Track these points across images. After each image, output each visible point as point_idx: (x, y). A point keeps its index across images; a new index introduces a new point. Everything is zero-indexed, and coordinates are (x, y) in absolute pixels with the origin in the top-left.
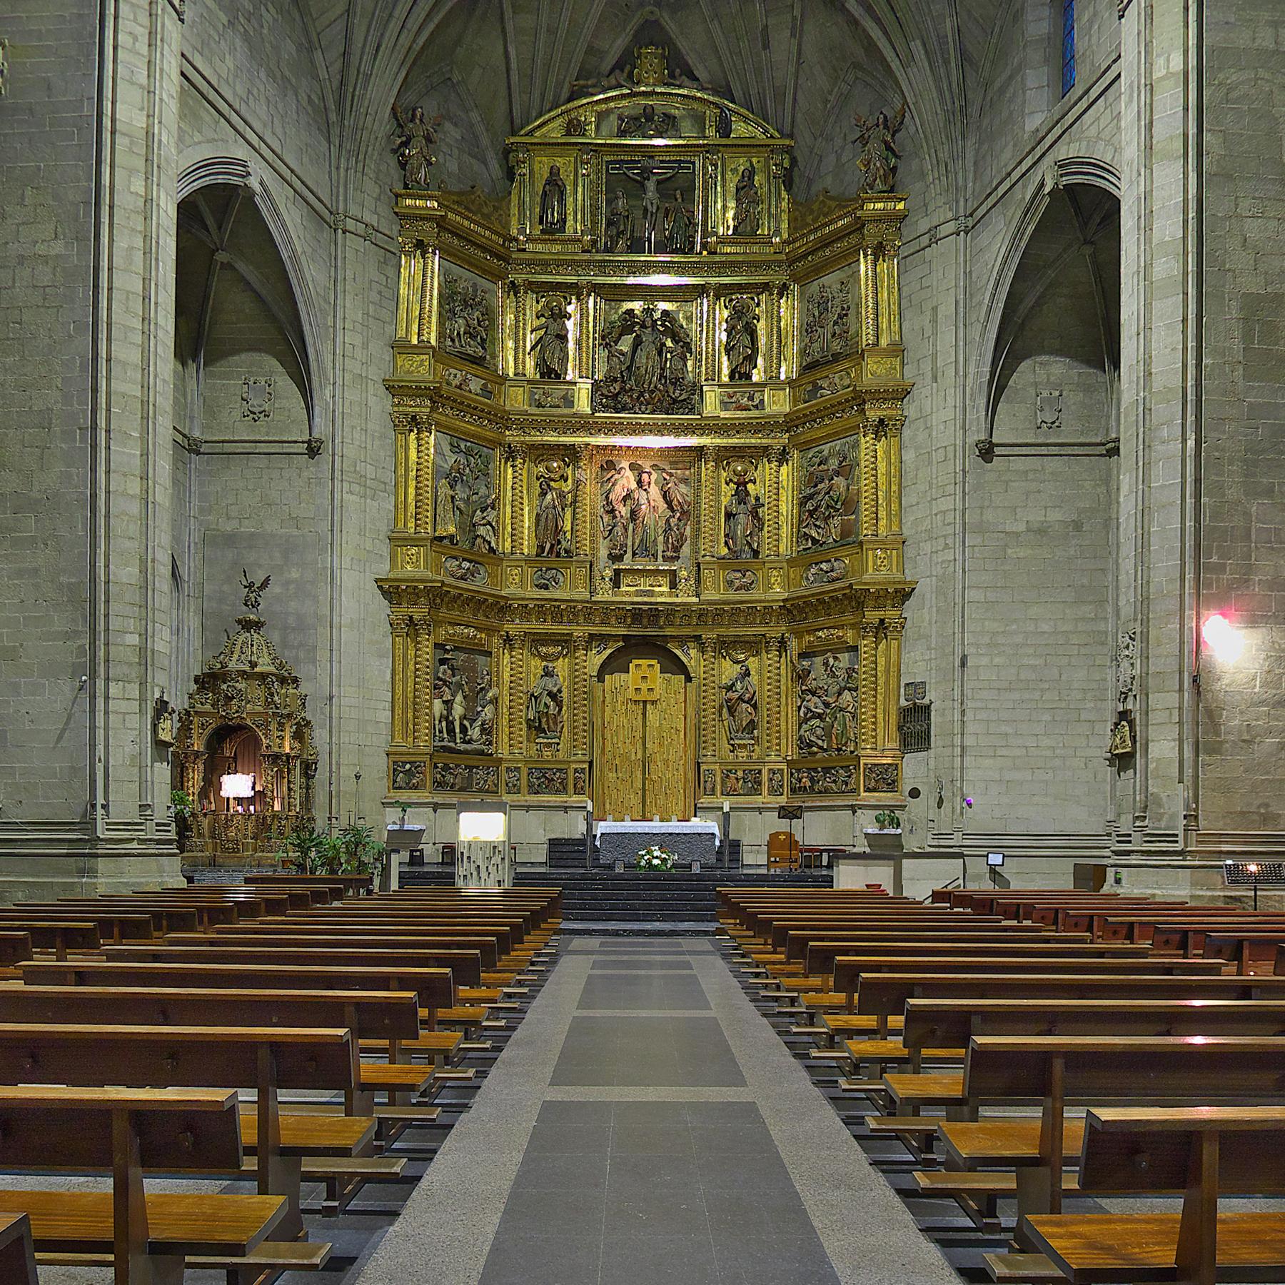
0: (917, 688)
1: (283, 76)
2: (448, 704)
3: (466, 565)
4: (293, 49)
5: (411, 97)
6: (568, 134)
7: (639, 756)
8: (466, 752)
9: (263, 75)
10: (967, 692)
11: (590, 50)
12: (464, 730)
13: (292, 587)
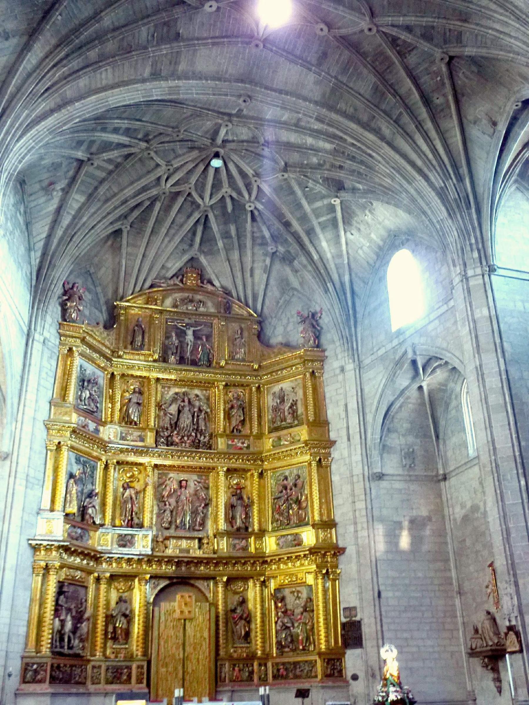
2: (63, 623)
3: (79, 531)
5: (72, 277)
6: (147, 303)
7: (181, 656)
8: (69, 655)
10: (383, 613)
11: (163, 267)
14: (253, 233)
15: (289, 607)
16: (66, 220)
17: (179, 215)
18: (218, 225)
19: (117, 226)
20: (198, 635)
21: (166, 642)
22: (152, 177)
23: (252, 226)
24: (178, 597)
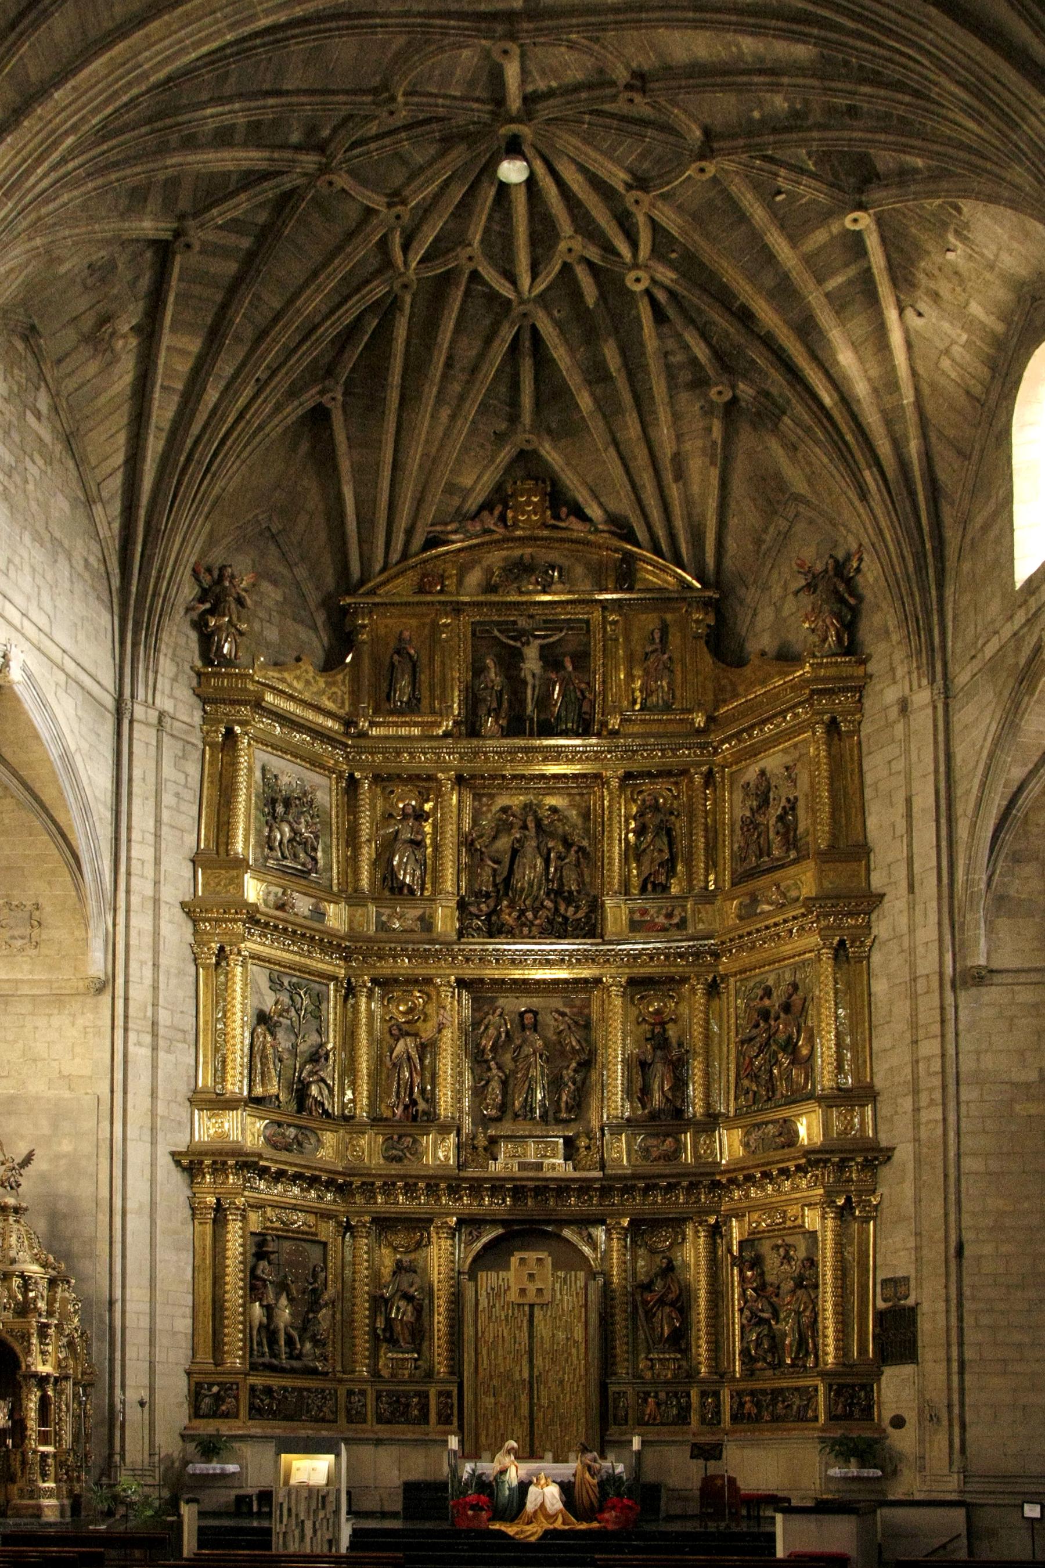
0: (895, 1285)
1: (53, 539)
4: (65, 506)
8: (293, 1371)
9: (27, 538)
12: (290, 1341)
13: (63, 1162)
14: (666, 354)
15: (770, 1278)
16: (163, 411)
17: (464, 342)
18: (572, 351)
19: (309, 398)
20: (561, 1335)
21: (493, 1347)
22: (362, 250)
23: (660, 337)
24: (514, 1260)
